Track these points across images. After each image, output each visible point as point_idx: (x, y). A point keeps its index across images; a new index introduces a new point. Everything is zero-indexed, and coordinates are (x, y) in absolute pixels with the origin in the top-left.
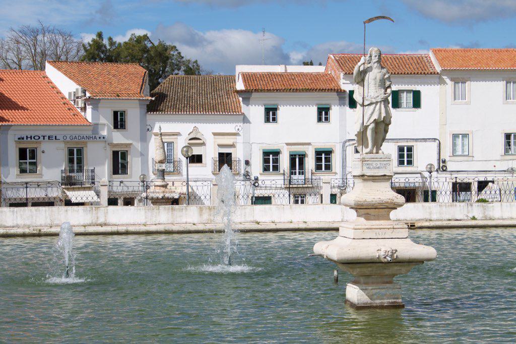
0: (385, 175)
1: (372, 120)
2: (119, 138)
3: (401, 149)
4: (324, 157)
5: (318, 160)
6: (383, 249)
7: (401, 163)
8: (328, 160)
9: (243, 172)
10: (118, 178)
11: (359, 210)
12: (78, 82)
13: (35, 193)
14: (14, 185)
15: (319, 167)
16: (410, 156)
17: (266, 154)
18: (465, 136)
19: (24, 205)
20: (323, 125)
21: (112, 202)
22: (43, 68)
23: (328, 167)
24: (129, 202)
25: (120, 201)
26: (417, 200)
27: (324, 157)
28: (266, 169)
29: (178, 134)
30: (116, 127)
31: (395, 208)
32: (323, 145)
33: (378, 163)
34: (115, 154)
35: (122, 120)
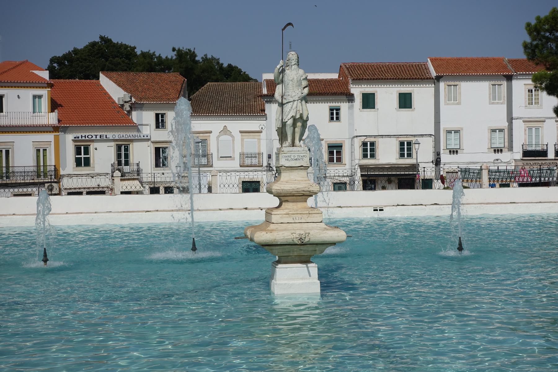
0: (302, 166)
1: (290, 116)
3: (402, 144)
4: (335, 151)
5: (331, 153)
6: (298, 232)
7: (365, 156)
8: (339, 153)
9: (265, 164)
10: (160, 170)
11: (281, 198)
12: (125, 89)
13: (92, 183)
14: (70, 176)
15: (331, 160)
16: (402, 149)
18: (457, 132)
19: (80, 193)
20: (335, 124)
21: (154, 191)
22: (98, 78)
23: (339, 160)
24: (169, 190)
25: (162, 190)
26: (416, 187)
27: (335, 151)
29: (210, 132)
30: (157, 127)
31: (312, 196)
32: (334, 139)
33: (296, 155)
34: (157, 150)
35: (162, 121)
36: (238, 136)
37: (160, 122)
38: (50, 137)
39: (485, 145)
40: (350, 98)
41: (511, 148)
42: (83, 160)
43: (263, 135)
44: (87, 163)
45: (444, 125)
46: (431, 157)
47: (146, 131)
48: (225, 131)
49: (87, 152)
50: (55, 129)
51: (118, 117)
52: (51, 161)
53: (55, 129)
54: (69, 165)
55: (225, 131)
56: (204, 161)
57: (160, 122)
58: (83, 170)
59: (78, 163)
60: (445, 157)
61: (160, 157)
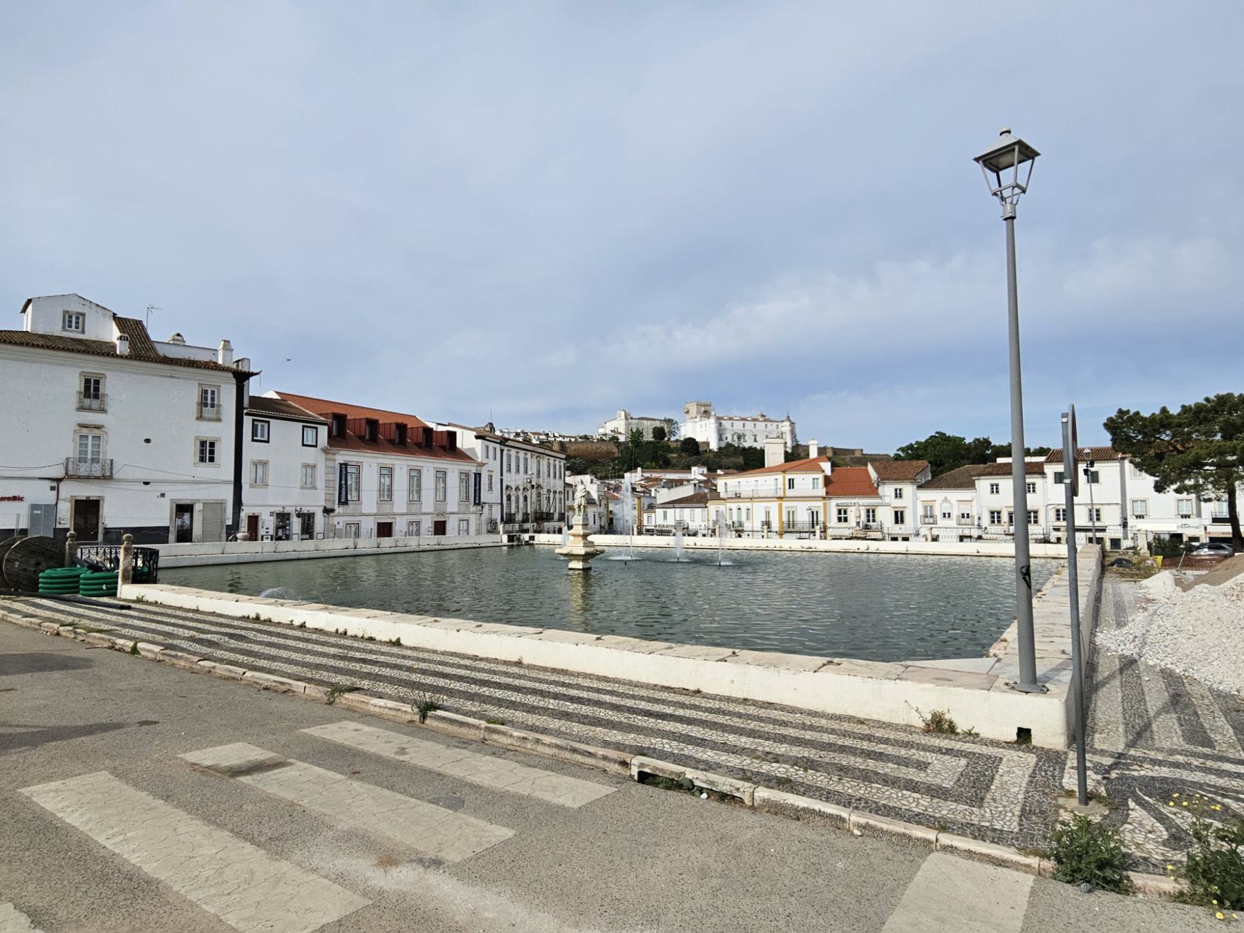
2: (898, 503)
17: (992, 513)
21: (895, 539)
23: (1036, 522)
28: (993, 522)
36: (955, 504)
37: (898, 494)
38: (821, 504)
39: (1174, 511)
40: (1042, 474)
41: (1199, 515)
42: (843, 518)
43: (974, 503)
44: (846, 519)
45: (1130, 496)
46: (1119, 521)
47: (887, 500)
48: (946, 500)
49: (845, 512)
50: (824, 498)
51: (872, 491)
52: (821, 518)
53: (824, 498)
54: (833, 521)
55: (946, 500)
56: (931, 520)
57: (898, 494)
58: (843, 524)
59: (840, 520)
60: (1131, 521)
61: (899, 517)
